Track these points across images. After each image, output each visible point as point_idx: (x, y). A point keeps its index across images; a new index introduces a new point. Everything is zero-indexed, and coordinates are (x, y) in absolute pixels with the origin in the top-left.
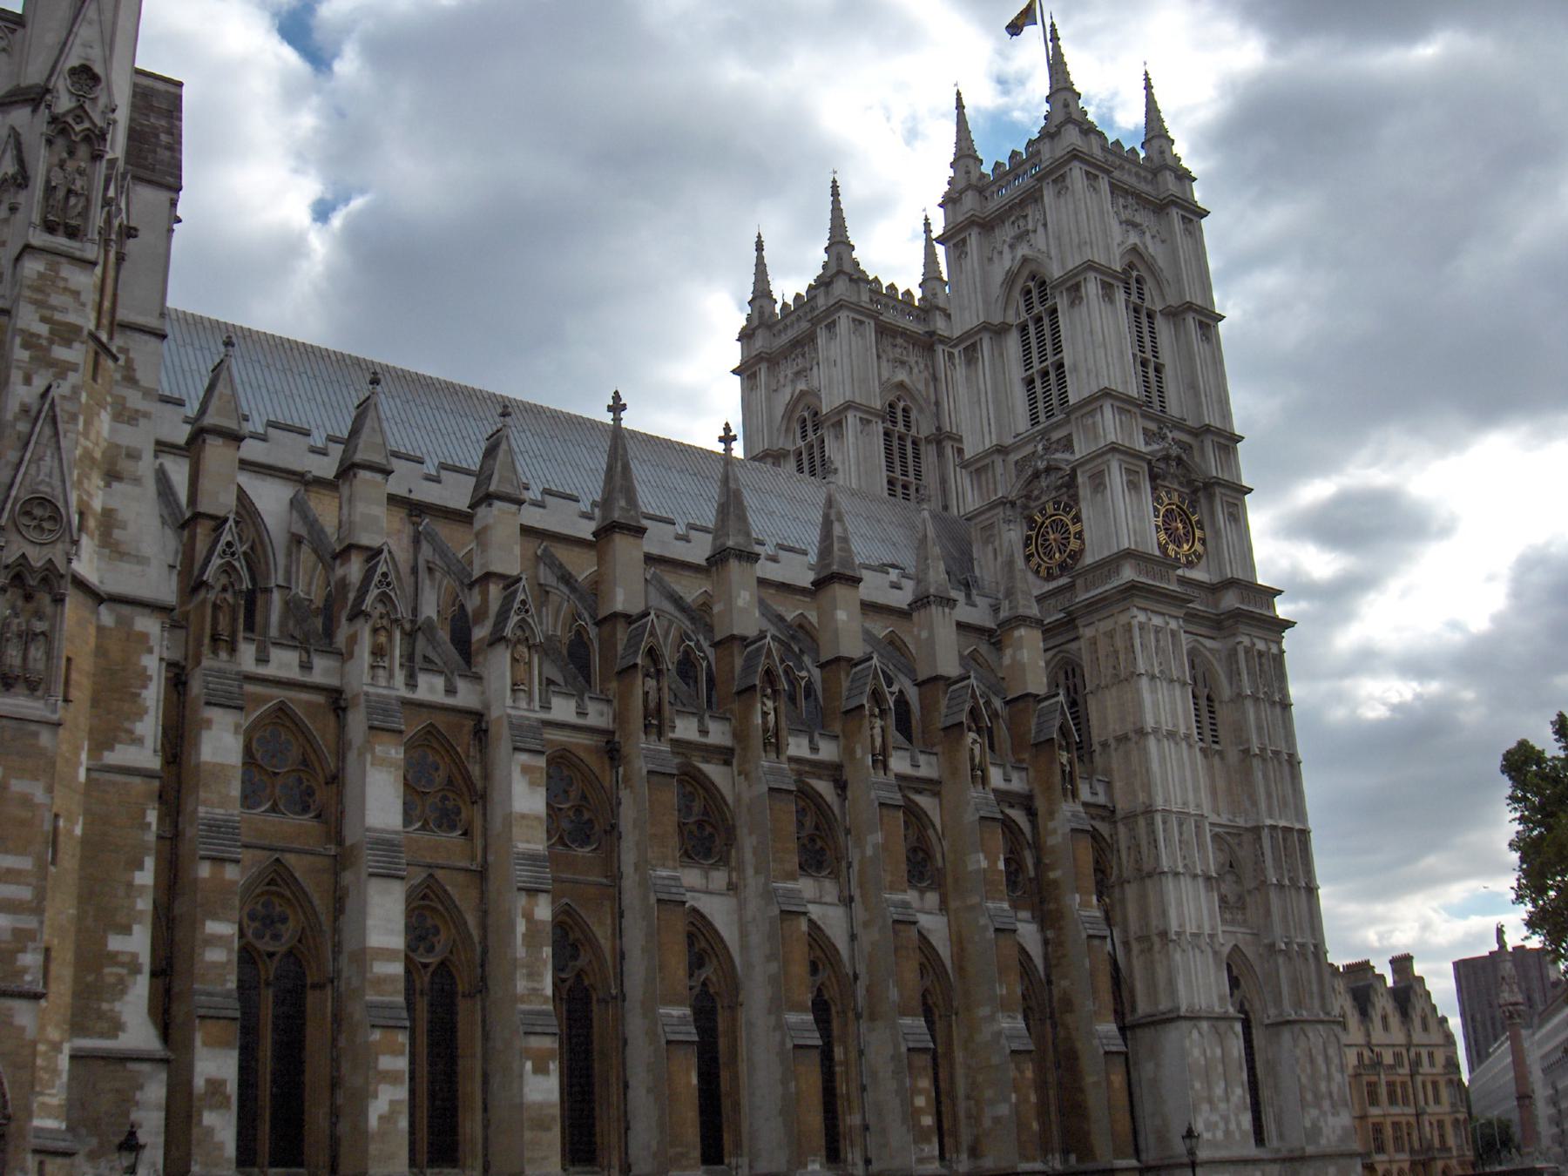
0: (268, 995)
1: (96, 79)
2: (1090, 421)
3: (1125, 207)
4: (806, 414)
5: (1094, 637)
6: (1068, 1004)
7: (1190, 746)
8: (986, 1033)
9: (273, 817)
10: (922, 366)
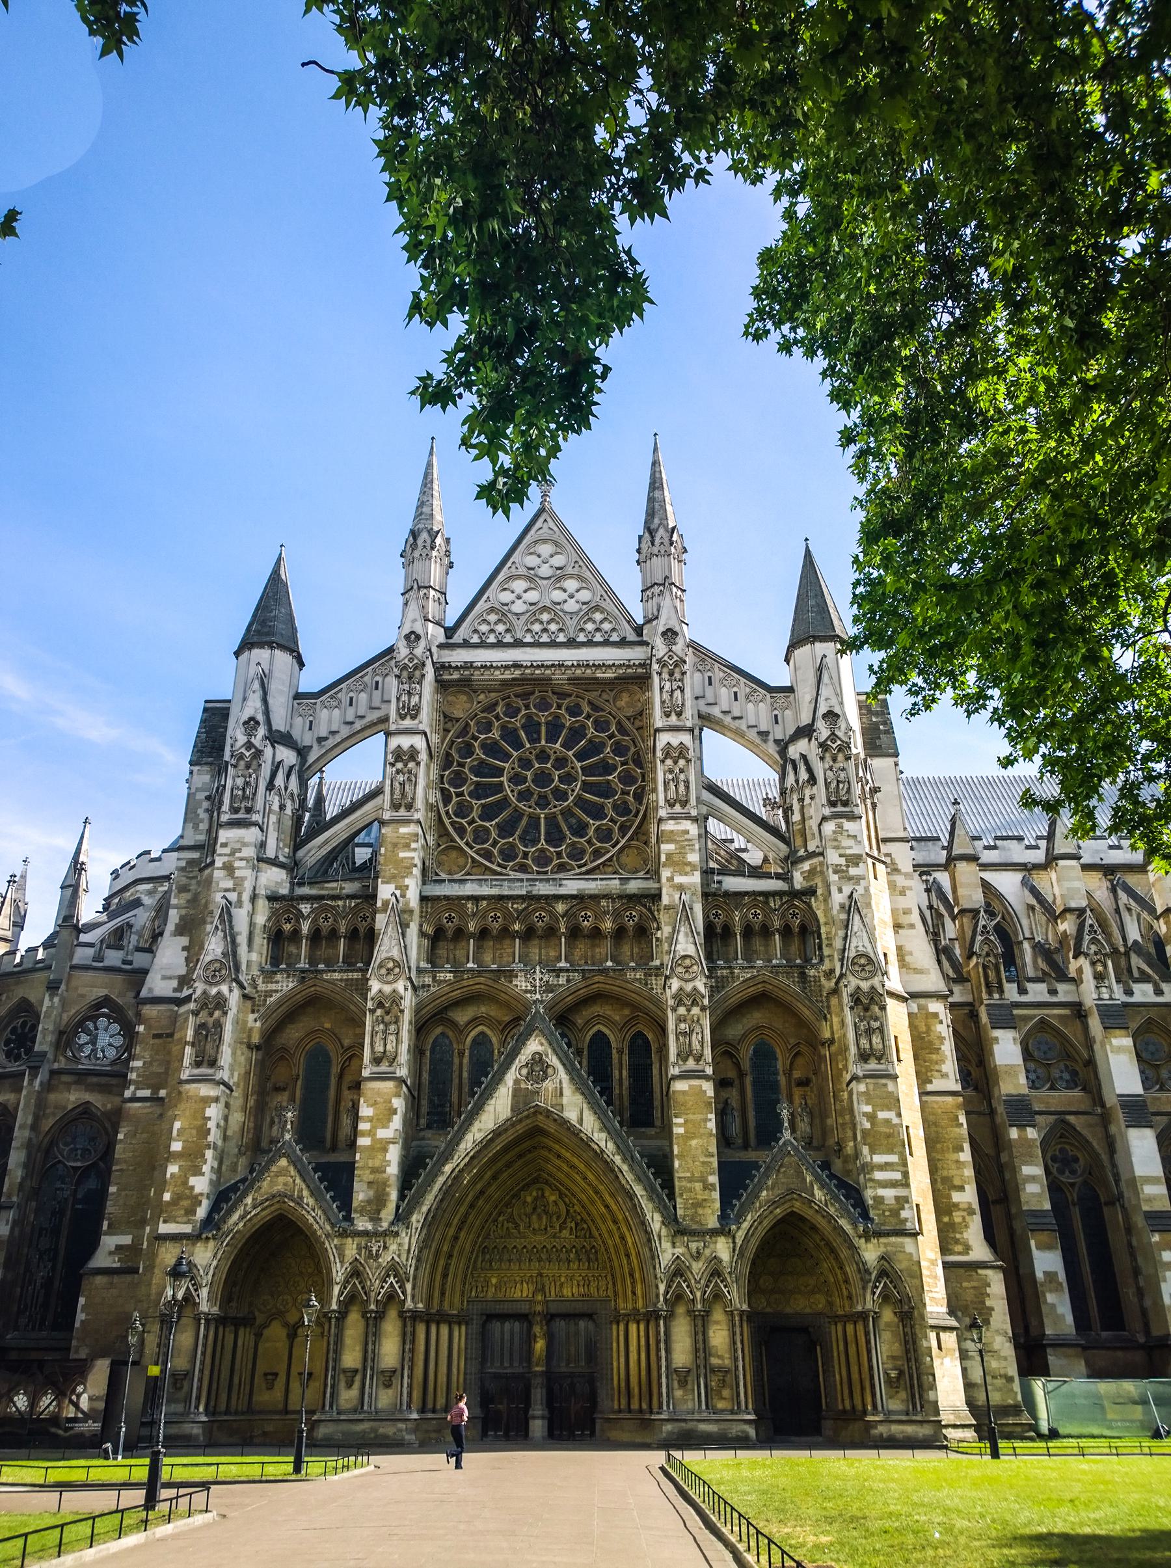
0: (1076, 1213)
1: (837, 716)
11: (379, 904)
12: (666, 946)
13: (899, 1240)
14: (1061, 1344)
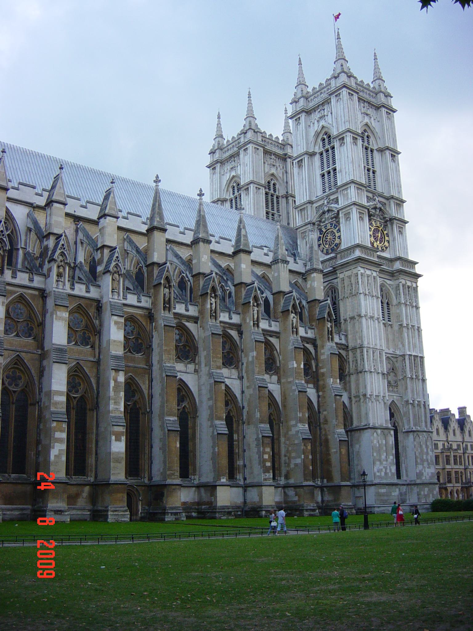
2: (346, 192)
3: (364, 107)
4: (235, 184)
5: (343, 278)
6: (326, 421)
7: (379, 322)
8: (293, 431)
9: (18, 339)
10: (282, 167)
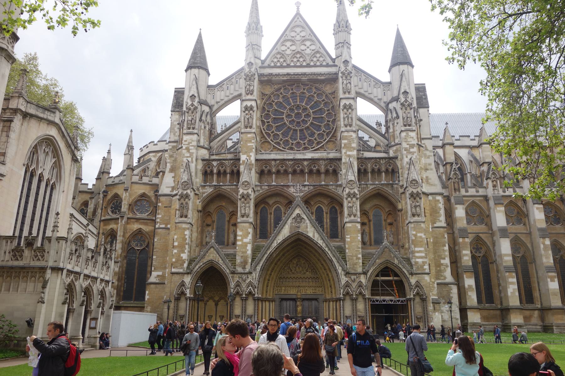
0: (480, 266)
1: (408, 93)
9: (475, 226)
11: (241, 162)
12: (344, 177)
13: (423, 275)
14: (472, 308)
